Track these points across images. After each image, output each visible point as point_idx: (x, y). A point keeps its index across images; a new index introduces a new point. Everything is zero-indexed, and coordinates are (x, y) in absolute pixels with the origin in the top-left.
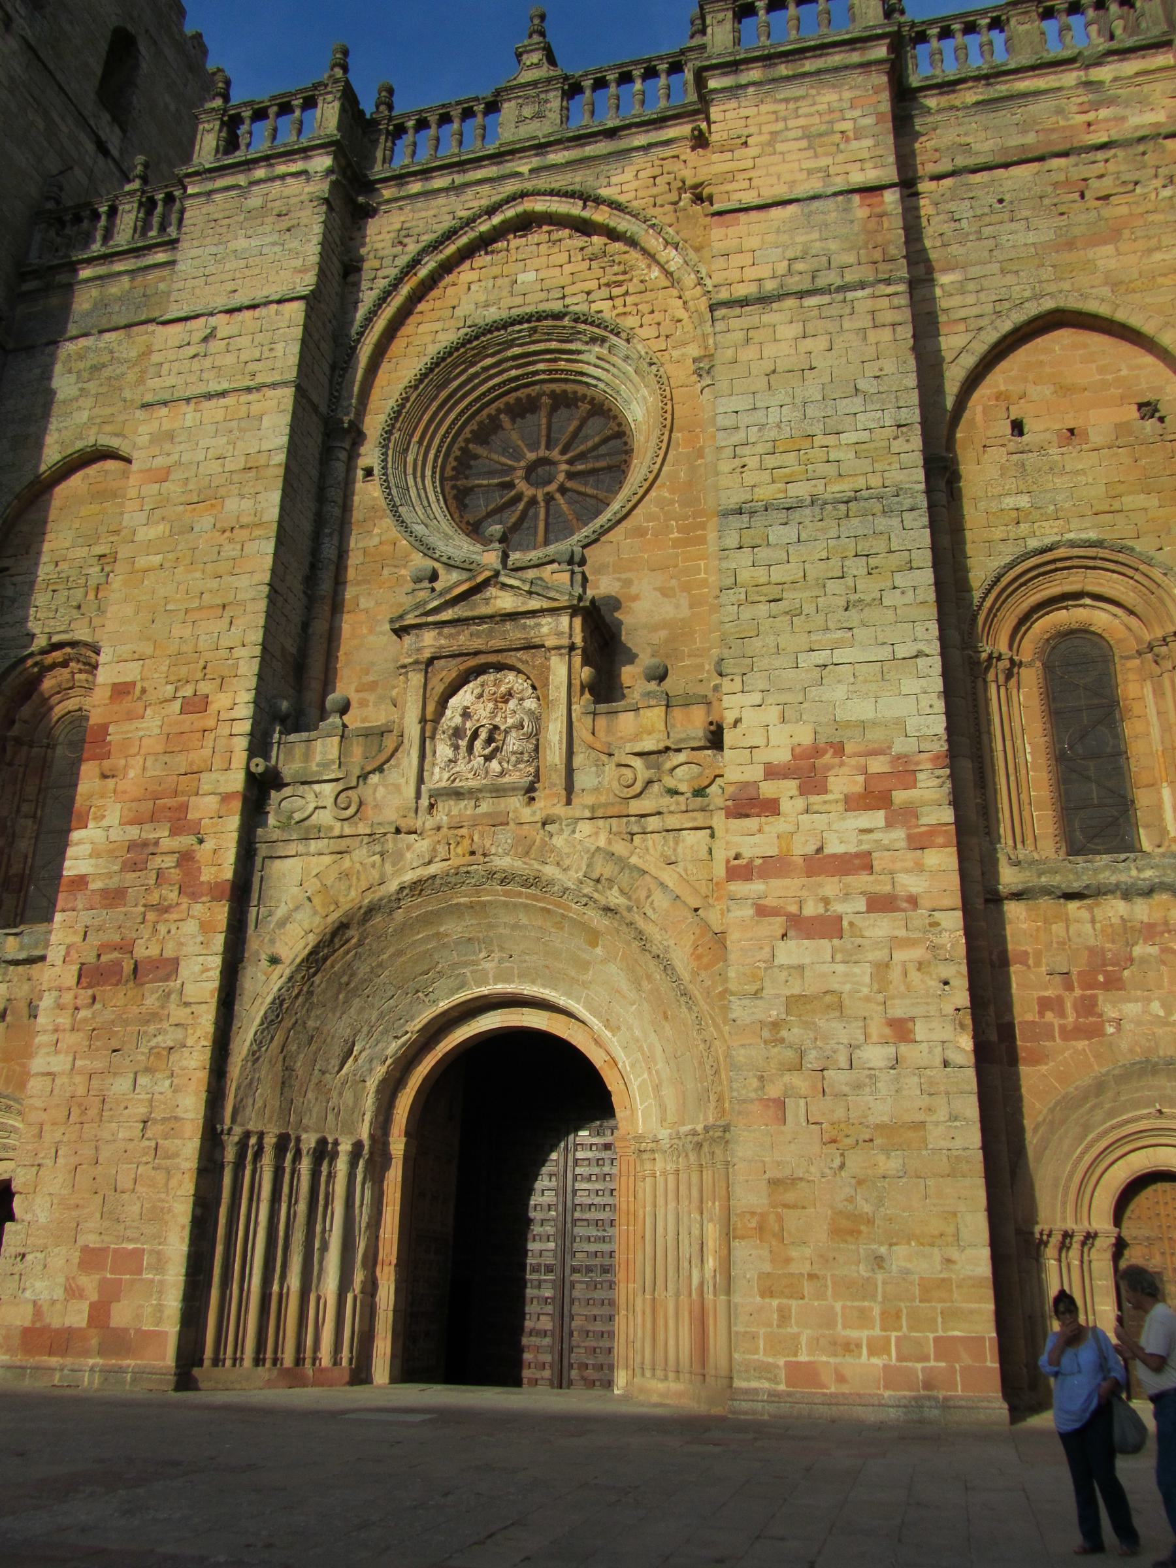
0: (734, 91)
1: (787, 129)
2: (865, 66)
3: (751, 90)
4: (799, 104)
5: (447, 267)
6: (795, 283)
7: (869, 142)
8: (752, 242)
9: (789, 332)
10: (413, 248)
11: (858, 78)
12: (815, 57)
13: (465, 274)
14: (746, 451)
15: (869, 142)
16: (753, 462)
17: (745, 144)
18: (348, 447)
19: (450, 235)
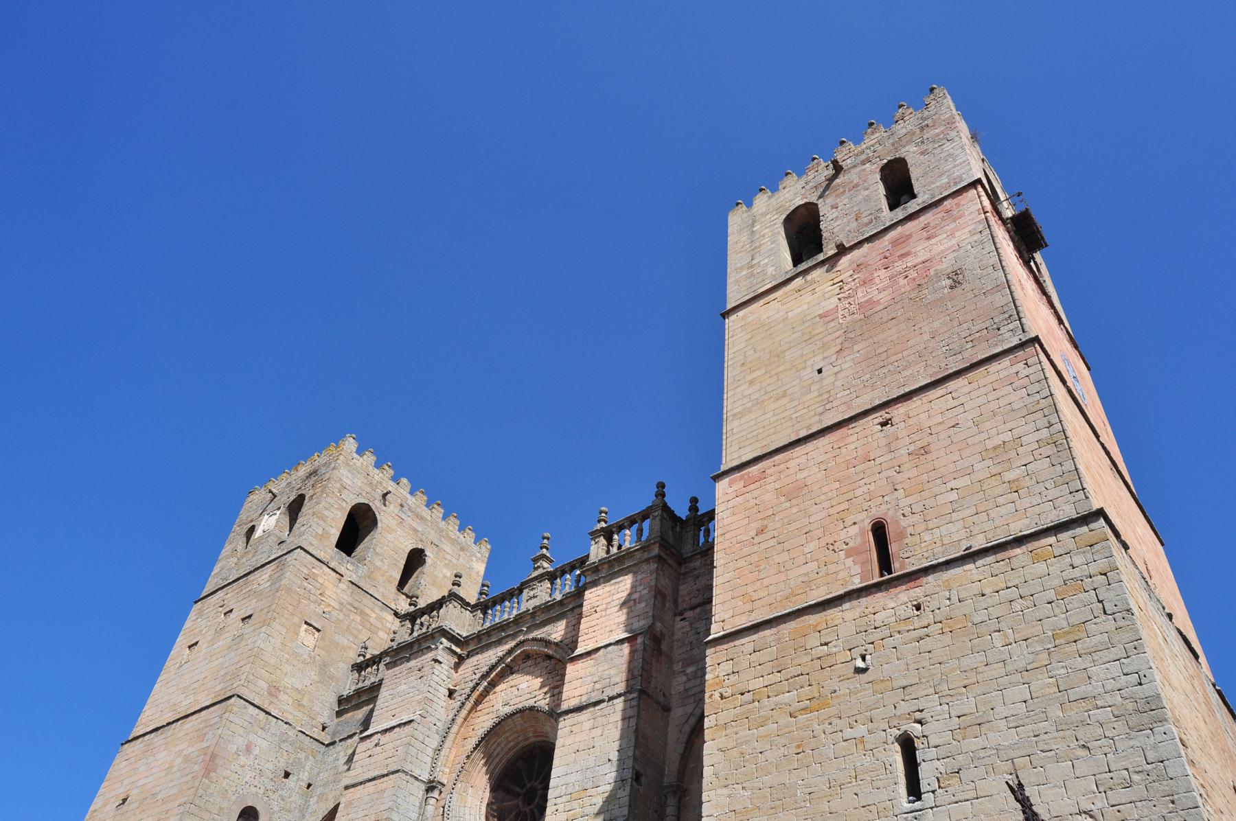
0: (595, 584)
1: (613, 601)
2: (647, 561)
3: (601, 580)
4: (620, 585)
5: (493, 685)
6: (595, 697)
7: (643, 604)
8: (581, 673)
9: (587, 725)
10: (478, 675)
11: (645, 567)
12: (629, 557)
13: (498, 688)
14: (558, 801)
15: (643, 604)
16: (560, 807)
17: (596, 611)
18: (437, 796)
19: (492, 668)
